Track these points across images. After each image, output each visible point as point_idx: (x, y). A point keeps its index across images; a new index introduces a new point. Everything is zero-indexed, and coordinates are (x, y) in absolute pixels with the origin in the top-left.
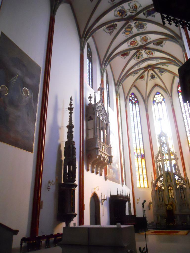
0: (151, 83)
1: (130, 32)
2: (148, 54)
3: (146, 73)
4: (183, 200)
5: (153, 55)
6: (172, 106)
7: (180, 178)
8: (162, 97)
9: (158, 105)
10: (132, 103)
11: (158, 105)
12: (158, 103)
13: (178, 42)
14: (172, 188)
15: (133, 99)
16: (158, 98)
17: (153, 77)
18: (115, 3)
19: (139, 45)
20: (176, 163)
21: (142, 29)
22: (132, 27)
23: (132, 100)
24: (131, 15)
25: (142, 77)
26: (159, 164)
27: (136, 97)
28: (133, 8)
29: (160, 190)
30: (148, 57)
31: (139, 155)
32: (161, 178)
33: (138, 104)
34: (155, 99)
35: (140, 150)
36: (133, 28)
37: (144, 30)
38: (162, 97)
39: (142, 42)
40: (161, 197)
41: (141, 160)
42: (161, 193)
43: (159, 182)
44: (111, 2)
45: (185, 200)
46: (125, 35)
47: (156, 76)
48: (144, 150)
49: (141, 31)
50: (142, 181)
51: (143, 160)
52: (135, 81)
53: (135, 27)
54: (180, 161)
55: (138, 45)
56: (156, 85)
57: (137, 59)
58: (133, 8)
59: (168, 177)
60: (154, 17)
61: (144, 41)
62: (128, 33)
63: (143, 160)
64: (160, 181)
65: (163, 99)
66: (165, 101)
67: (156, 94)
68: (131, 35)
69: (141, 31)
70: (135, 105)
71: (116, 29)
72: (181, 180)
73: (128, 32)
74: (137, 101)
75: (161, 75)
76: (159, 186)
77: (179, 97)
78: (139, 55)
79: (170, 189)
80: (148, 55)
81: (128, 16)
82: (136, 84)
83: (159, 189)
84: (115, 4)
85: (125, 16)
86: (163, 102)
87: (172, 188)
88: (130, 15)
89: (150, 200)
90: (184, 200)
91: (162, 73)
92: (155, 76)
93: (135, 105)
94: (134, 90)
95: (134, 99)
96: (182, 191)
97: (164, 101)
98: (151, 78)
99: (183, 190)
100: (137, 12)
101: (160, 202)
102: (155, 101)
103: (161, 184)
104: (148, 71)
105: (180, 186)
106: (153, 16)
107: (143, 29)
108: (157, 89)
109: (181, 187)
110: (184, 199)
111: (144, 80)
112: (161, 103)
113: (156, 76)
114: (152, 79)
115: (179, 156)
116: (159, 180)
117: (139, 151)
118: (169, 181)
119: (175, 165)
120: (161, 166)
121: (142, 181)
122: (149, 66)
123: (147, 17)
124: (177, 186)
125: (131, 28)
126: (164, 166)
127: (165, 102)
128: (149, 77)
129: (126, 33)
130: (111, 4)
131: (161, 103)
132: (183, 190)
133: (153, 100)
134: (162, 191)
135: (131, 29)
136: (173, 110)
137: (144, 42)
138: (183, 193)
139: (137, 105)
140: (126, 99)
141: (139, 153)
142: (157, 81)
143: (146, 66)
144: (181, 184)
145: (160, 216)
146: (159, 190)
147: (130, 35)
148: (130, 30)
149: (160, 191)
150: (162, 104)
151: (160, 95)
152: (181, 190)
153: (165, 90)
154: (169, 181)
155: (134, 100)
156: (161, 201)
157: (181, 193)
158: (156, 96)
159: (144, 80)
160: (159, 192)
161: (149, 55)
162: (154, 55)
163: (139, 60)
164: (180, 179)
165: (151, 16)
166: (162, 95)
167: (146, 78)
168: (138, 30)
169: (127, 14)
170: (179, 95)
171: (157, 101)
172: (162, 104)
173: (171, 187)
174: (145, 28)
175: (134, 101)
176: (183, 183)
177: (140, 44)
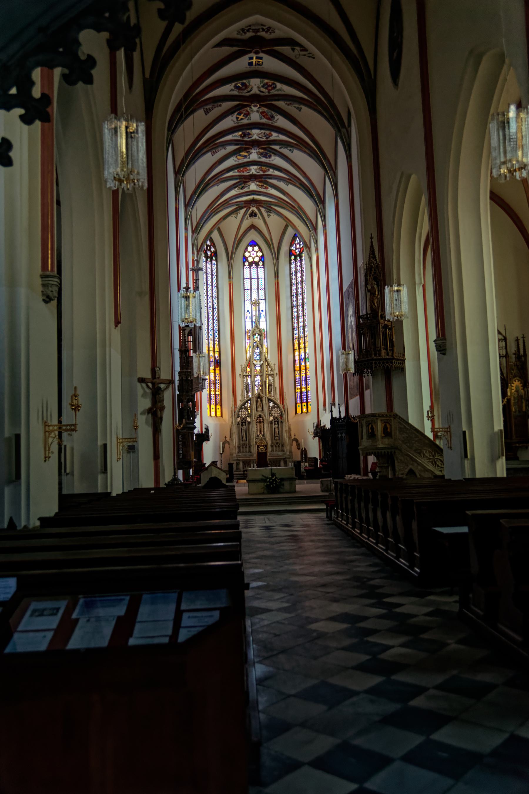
0: (246, 223)
1: (245, 157)
2: (261, 186)
3: (243, 211)
4: (276, 438)
5: (268, 190)
6: (277, 276)
7: (276, 406)
8: (260, 254)
9: (250, 268)
10: (206, 257)
11: (250, 268)
12: (251, 264)
13: (318, 206)
14: (262, 421)
15: (209, 248)
16: (253, 254)
17: (253, 215)
18: (242, 123)
19: (251, 173)
20: (273, 382)
21: (266, 158)
22: (252, 152)
23: (206, 251)
24: (258, 139)
25: (235, 211)
26: (247, 380)
27: (213, 244)
28: (266, 134)
29: (244, 422)
30: (258, 190)
31: (212, 359)
33: (216, 260)
34: (247, 254)
35: (214, 351)
36: (253, 154)
37: (270, 161)
38: (260, 254)
39: (258, 171)
40: (244, 434)
41: (215, 370)
42: (244, 427)
43: (243, 410)
44: (236, 121)
45: (279, 438)
46: (236, 159)
47: (259, 215)
48: (219, 352)
49: (263, 159)
50: (213, 406)
51: (217, 372)
52: (221, 219)
53: (256, 153)
54: (277, 379)
55: (249, 172)
56: (252, 227)
57: (238, 189)
58: (266, 134)
59: (259, 403)
60: (292, 152)
61: (261, 171)
62: (242, 158)
63: (216, 369)
64: (245, 409)
65: (262, 258)
66: (263, 262)
67: (249, 245)
68: (246, 160)
69: (263, 159)
70: (211, 261)
71: (225, 149)
72: (277, 409)
73: (243, 156)
74: (215, 254)
75: (269, 216)
76: (244, 416)
77: (290, 263)
78: (245, 185)
79: (260, 422)
80: (260, 187)
81: (253, 139)
82: (222, 225)
83: (242, 420)
84: (240, 124)
85: (249, 138)
86: (261, 263)
87: (262, 421)
88: (255, 139)
89: (226, 438)
90: (278, 438)
91: (271, 214)
92: (257, 216)
93: (211, 261)
94: (215, 235)
95: (210, 248)
96: (277, 426)
97: (262, 261)
98: (249, 216)
99: (278, 424)
100: (269, 139)
101: (242, 440)
102: (245, 259)
103: (247, 413)
104: (250, 208)
105: (275, 418)
106: (291, 150)
107: (269, 159)
108: (253, 235)
109: (276, 420)
110: (277, 437)
111: (236, 217)
112: (257, 264)
113: (259, 215)
114: (250, 218)
115: (277, 371)
116: (243, 406)
117: (211, 354)
118: (260, 409)
120: (250, 383)
121: (213, 406)
122: (253, 201)
123: (280, 148)
124: (271, 417)
125: (249, 153)
126: (254, 384)
127: (263, 265)
128: (248, 215)
129: (238, 157)
130: (234, 123)
131: (257, 264)
132: (278, 424)
134: (247, 425)
135: (249, 155)
136: (277, 285)
137: (260, 172)
138: (278, 428)
139: (214, 262)
140: (198, 252)
141: (212, 356)
142: (258, 222)
143: (248, 200)
144: (276, 415)
145: (243, 462)
146: (242, 422)
147: (242, 160)
148: (246, 154)
149: (244, 424)
150: (257, 268)
151: (256, 249)
152: (275, 424)
153: (269, 244)
154: (260, 409)
155: (210, 250)
156: (243, 439)
157: (275, 429)
158: (250, 249)
160: (242, 425)
161: (260, 189)
162: (269, 191)
163: (242, 191)
164: (276, 407)
165: (288, 149)
166: (260, 250)
167: (240, 216)
168: (259, 158)
169: (252, 137)
170: (290, 260)
171: (250, 260)
172: (257, 268)
173: (261, 419)
174: (271, 159)
175: (209, 253)
176: (280, 414)
177: (253, 173)
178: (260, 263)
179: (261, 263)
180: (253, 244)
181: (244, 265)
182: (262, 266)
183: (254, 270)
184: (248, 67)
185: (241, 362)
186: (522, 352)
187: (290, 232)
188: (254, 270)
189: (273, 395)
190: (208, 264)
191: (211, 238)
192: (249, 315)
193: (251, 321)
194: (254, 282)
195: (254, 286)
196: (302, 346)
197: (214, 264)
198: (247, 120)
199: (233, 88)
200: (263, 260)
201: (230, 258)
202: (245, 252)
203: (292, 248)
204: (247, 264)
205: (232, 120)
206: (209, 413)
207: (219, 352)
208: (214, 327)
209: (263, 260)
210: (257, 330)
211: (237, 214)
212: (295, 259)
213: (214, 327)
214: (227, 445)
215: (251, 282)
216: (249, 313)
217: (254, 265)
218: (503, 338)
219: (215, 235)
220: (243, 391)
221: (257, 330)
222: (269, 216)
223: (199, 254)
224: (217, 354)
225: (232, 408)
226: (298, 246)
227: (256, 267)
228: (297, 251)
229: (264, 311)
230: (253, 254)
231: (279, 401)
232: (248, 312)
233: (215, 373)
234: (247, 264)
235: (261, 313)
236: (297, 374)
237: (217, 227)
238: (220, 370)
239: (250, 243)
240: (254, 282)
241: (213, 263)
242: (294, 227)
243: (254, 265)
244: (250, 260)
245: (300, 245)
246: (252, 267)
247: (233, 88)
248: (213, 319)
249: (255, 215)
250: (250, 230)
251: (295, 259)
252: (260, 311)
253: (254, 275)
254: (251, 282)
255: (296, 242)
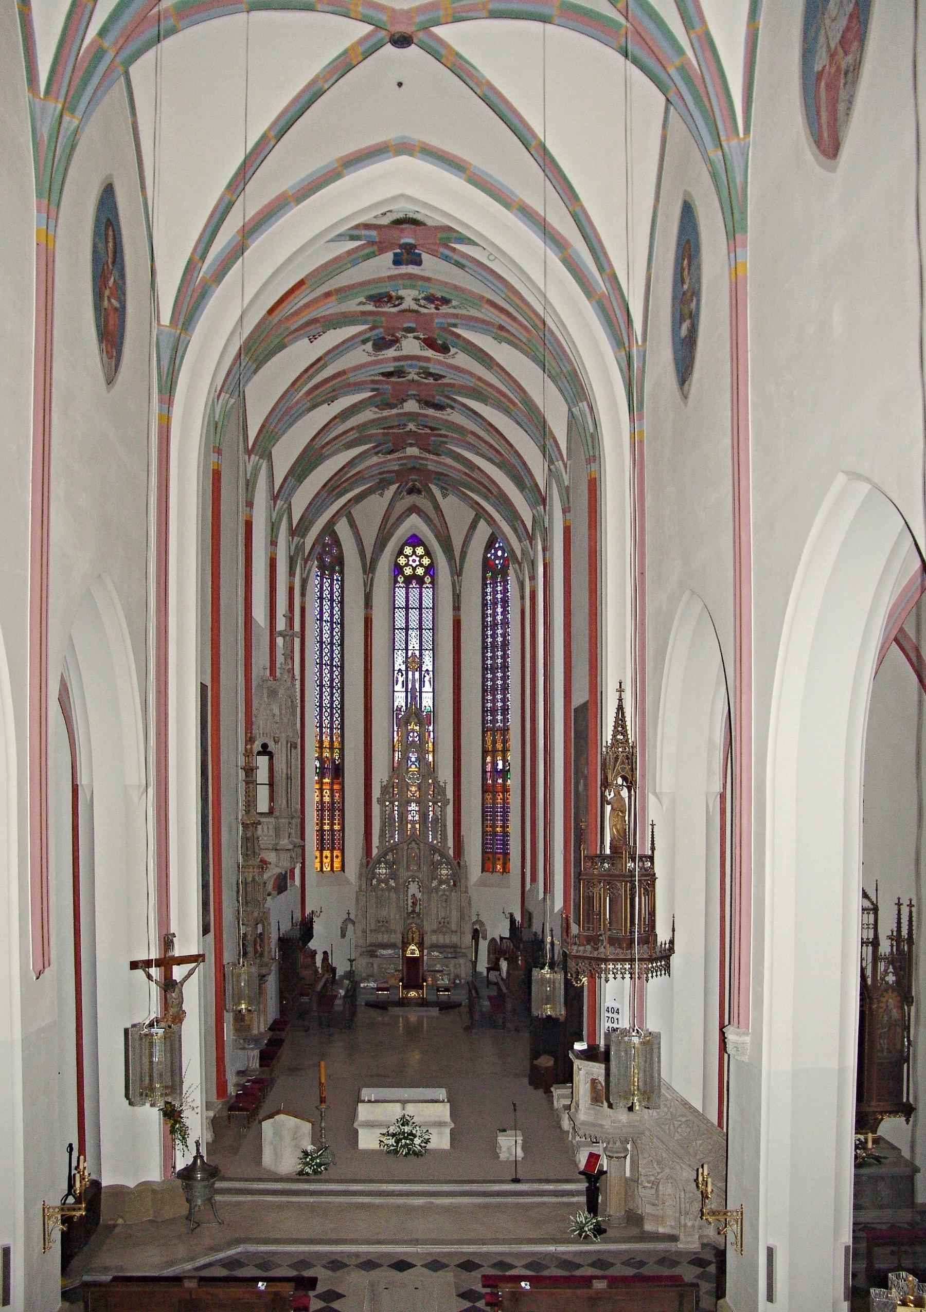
8: (426, 561)
10: (322, 567)
12: (408, 580)
19: (408, 429)
27: (337, 542)
30: (424, 456)
32: (390, 854)
34: (402, 561)
38: (426, 561)
41: (332, 784)
43: (383, 865)
65: (430, 570)
67: (407, 543)
74: (340, 561)
75: (445, 496)
86: (428, 579)
97: (431, 576)
102: (398, 569)
111: (382, 495)
112: (420, 581)
119: (435, 820)
127: (432, 583)
131: (420, 581)
133: (396, 561)
151: (420, 551)
158: (408, 550)
159: (382, 495)
164: (444, 862)
171: (408, 571)
174: (445, 412)
178: (426, 579)
179: (428, 579)
180: (415, 541)
181: (396, 582)
182: (430, 586)
183: (414, 593)
184: (393, 267)
185: (380, 775)
186: (905, 932)
187: (483, 531)
188: (414, 593)
189: (440, 840)
190: (325, 580)
191: (334, 532)
192: (401, 679)
193: (404, 690)
194: (414, 615)
195: (414, 623)
196: (499, 746)
197: (337, 580)
198: (395, 350)
199: (364, 300)
200: (431, 573)
201: (369, 568)
202: (398, 556)
203: (489, 555)
204: (401, 579)
205: (364, 350)
206: (318, 865)
207: (342, 750)
208: (332, 702)
209: (431, 573)
210: (414, 713)
211: (383, 490)
212: (494, 578)
213: (332, 702)
214: (350, 927)
215: (407, 614)
216: (402, 675)
217: (414, 582)
218: (871, 906)
219: (342, 529)
220: (382, 831)
221: (414, 713)
222: (445, 496)
223: (308, 566)
224: (336, 756)
225: (361, 861)
226: (500, 553)
227: (418, 586)
228: (497, 562)
229: (431, 673)
230: (414, 561)
231: (451, 852)
232: (400, 674)
233: (332, 790)
234: (401, 579)
235: (425, 676)
236: (489, 797)
237: (345, 511)
238: (342, 784)
239: (407, 540)
240: (414, 615)
241: (335, 578)
242: (491, 521)
243: (414, 582)
244: (408, 571)
245: (503, 553)
246: (411, 586)
247: (364, 300)
248: (331, 687)
249: (419, 492)
250: (408, 516)
251: (494, 578)
252: (423, 673)
253: (414, 602)
254: (407, 614)
255: (497, 545)
